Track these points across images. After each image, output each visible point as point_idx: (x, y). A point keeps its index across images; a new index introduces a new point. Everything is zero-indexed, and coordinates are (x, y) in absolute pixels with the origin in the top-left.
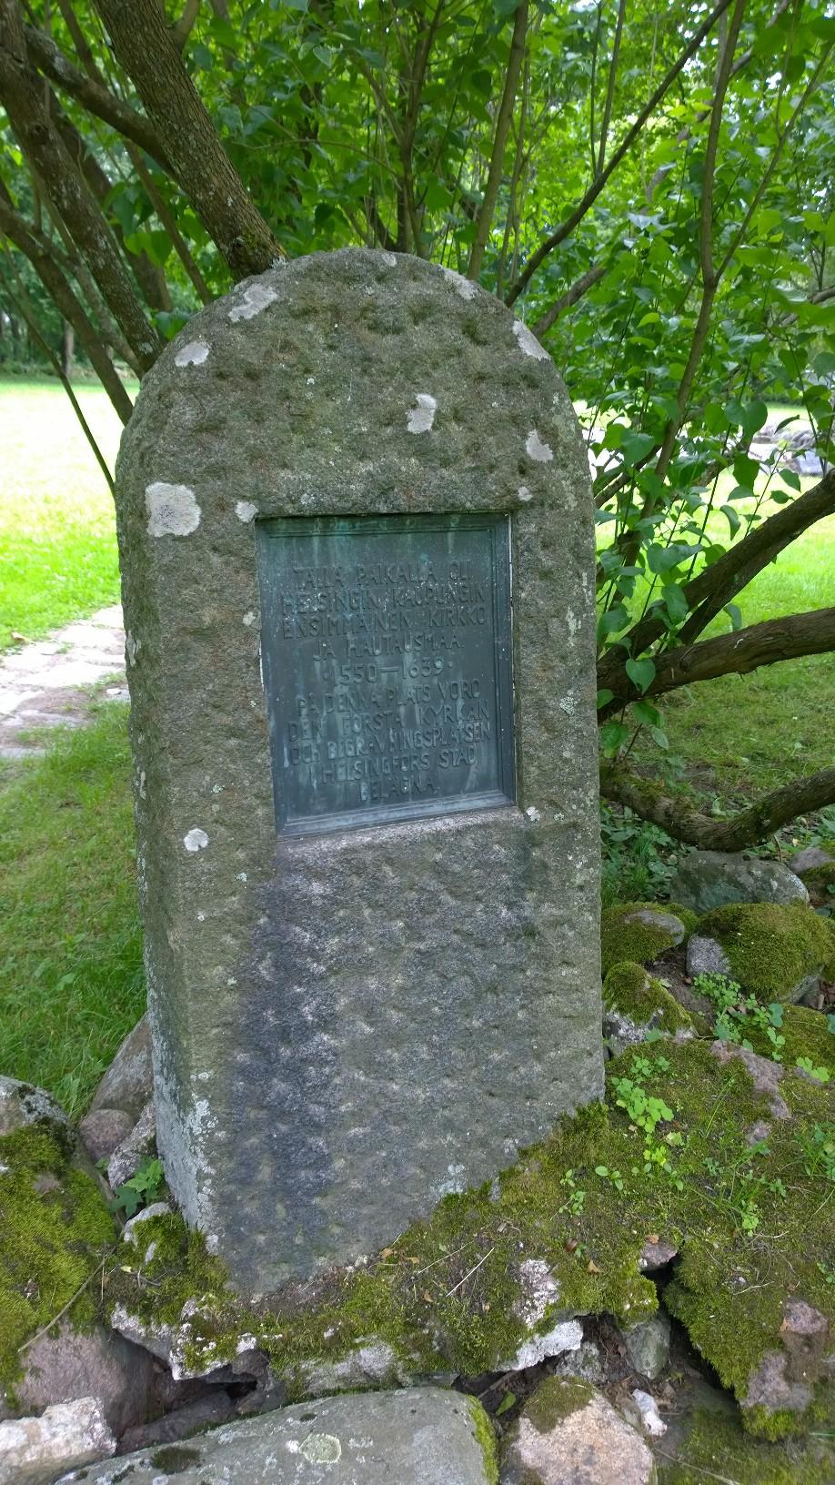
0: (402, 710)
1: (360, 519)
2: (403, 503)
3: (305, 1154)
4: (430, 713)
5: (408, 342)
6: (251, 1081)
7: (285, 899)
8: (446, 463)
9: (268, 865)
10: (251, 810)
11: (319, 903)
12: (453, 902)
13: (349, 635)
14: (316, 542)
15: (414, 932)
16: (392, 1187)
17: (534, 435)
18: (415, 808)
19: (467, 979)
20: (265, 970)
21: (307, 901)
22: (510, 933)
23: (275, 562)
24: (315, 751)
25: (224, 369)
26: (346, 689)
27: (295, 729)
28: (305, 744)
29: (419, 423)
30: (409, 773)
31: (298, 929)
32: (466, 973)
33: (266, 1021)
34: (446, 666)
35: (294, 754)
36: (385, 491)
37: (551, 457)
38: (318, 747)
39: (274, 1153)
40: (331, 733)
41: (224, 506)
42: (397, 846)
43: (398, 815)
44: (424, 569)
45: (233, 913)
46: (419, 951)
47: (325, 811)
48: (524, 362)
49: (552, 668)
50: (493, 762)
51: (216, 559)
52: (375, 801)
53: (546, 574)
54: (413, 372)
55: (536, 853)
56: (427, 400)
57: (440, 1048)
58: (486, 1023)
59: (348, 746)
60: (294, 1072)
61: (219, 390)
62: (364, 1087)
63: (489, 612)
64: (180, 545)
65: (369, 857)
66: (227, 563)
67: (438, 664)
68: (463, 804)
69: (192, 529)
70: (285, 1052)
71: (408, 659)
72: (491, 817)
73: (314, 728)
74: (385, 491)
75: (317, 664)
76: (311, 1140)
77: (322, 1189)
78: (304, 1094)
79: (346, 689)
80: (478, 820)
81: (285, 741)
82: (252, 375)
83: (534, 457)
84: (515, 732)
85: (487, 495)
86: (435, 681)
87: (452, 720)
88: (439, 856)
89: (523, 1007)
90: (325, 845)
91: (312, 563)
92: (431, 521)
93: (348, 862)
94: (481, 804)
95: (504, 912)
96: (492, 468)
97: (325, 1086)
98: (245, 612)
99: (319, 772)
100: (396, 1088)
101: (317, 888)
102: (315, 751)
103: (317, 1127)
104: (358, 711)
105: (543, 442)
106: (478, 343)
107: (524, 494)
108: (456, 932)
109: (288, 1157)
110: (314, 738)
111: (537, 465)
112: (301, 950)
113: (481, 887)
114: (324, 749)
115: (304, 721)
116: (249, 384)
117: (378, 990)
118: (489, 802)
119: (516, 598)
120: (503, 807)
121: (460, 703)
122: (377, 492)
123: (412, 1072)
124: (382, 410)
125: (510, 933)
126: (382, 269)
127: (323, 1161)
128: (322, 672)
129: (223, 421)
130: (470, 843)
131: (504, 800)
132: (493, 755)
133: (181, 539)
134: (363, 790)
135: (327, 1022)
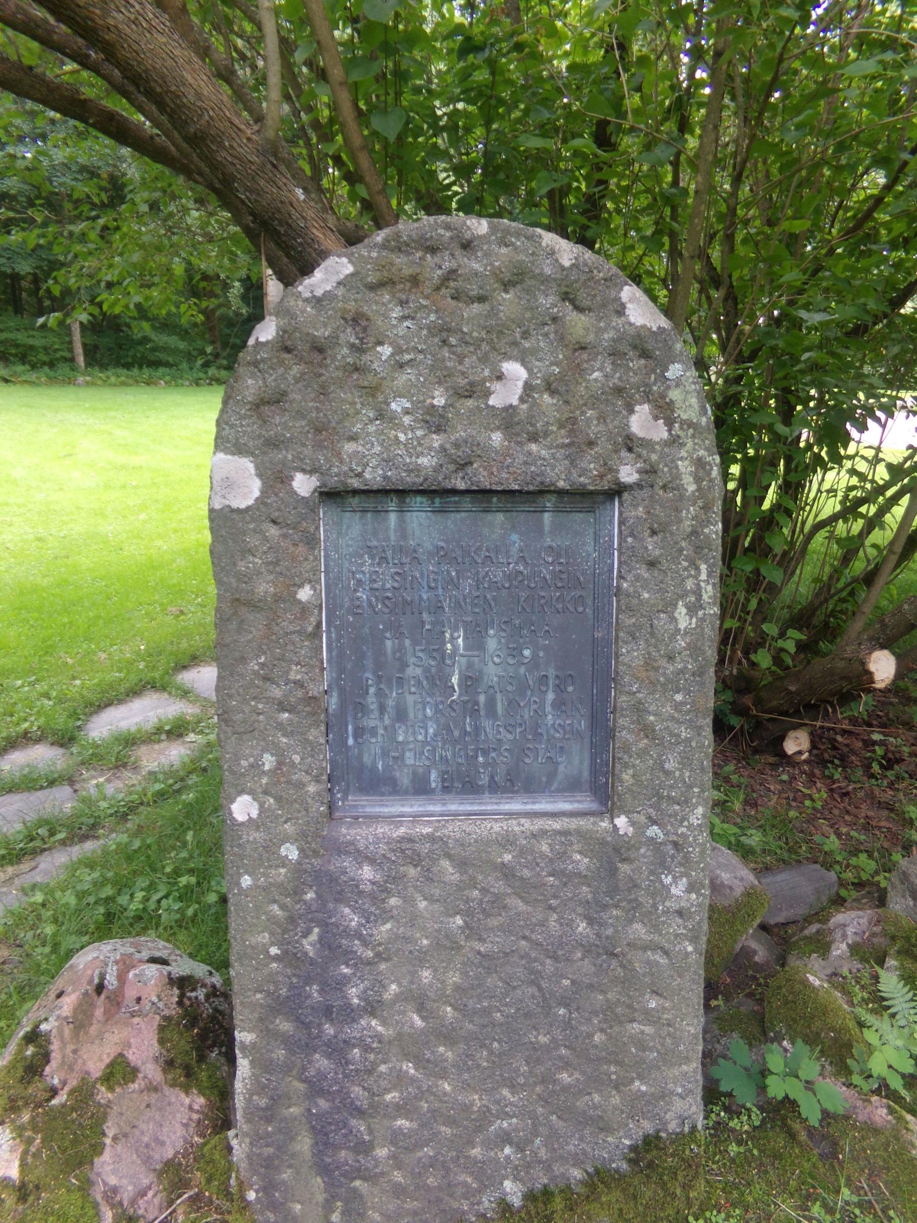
0: (482, 698)
1: (438, 495)
2: (485, 481)
3: (345, 1135)
4: (512, 704)
5: (493, 313)
6: (291, 1051)
7: (333, 880)
8: (533, 438)
9: (320, 843)
10: (300, 785)
11: (368, 888)
12: (521, 906)
13: (425, 616)
14: (393, 517)
15: (472, 931)
16: (439, 1188)
17: (643, 410)
18: (489, 804)
19: (532, 990)
20: (309, 945)
21: (355, 884)
22: (588, 950)
23: (342, 535)
24: (381, 731)
25: (289, 343)
26: (419, 671)
27: (362, 708)
28: (372, 724)
29: (505, 395)
30: (486, 765)
31: (347, 910)
32: (533, 983)
33: (309, 996)
34: (535, 655)
35: (359, 732)
36: (463, 466)
37: (665, 435)
38: (385, 728)
39: (313, 1128)
40: (401, 715)
41: (284, 479)
42: (461, 843)
43: (469, 808)
44: (514, 550)
45: (280, 886)
46: (479, 953)
47: (390, 794)
48: (632, 331)
49: (656, 669)
50: (586, 764)
51: (273, 531)
52: (446, 789)
53: (652, 564)
54: (500, 341)
55: (625, 868)
56: (515, 370)
57: (500, 1055)
58: (553, 1040)
59: (414, 733)
60: (338, 1050)
61: (281, 363)
62: (413, 1080)
63: (589, 602)
64: (235, 516)
65: (425, 848)
66: (285, 536)
67: (527, 653)
68: (543, 806)
69: (251, 502)
70: (329, 1029)
71: (492, 644)
72: (573, 824)
73: (382, 709)
74: (463, 466)
75: (389, 644)
76: (353, 1122)
77: (359, 1173)
78: (346, 1076)
79: (419, 671)
80: (557, 825)
81: (350, 719)
82: (319, 349)
83: (641, 434)
84: (611, 734)
85: (587, 473)
86: (522, 670)
87: (540, 713)
88: (507, 857)
89: (602, 1030)
90: (382, 829)
91: (387, 539)
92: (524, 498)
93: (403, 851)
94: (565, 806)
95: (582, 927)
96: (591, 444)
97: (370, 1072)
98: (301, 586)
99: (385, 754)
100: (447, 1087)
101: (367, 872)
102: (381, 731)
103: (360, 1113)
104: (431, 695)
105: (656, 418)
106: (579, 309)
107: (628, 474)
108: (524, 938)
109: (326, 1134)
110: (381, 719)
111: (646, 443)
112: (347, 932)
113: (555, 897)
114: (391, 732)
115: (371, 701)
116: (317, 357)
117: (431, 985)
118: (575, 806)
119: (619, 588)
120: (592, 814)
121: (551, 696)
122: (452, 467)
123: (466, 1076)
124: (462, 382)
125: (588, 950)
126: (468, 235)
127: (363, 1148)
128: (394, 653)
129: (284, 394)
130: (545, 848)
131: (594, 806)
132: (587, 755)
133: (238, 511)
134: (434, 775)
135: (372, 1008)
